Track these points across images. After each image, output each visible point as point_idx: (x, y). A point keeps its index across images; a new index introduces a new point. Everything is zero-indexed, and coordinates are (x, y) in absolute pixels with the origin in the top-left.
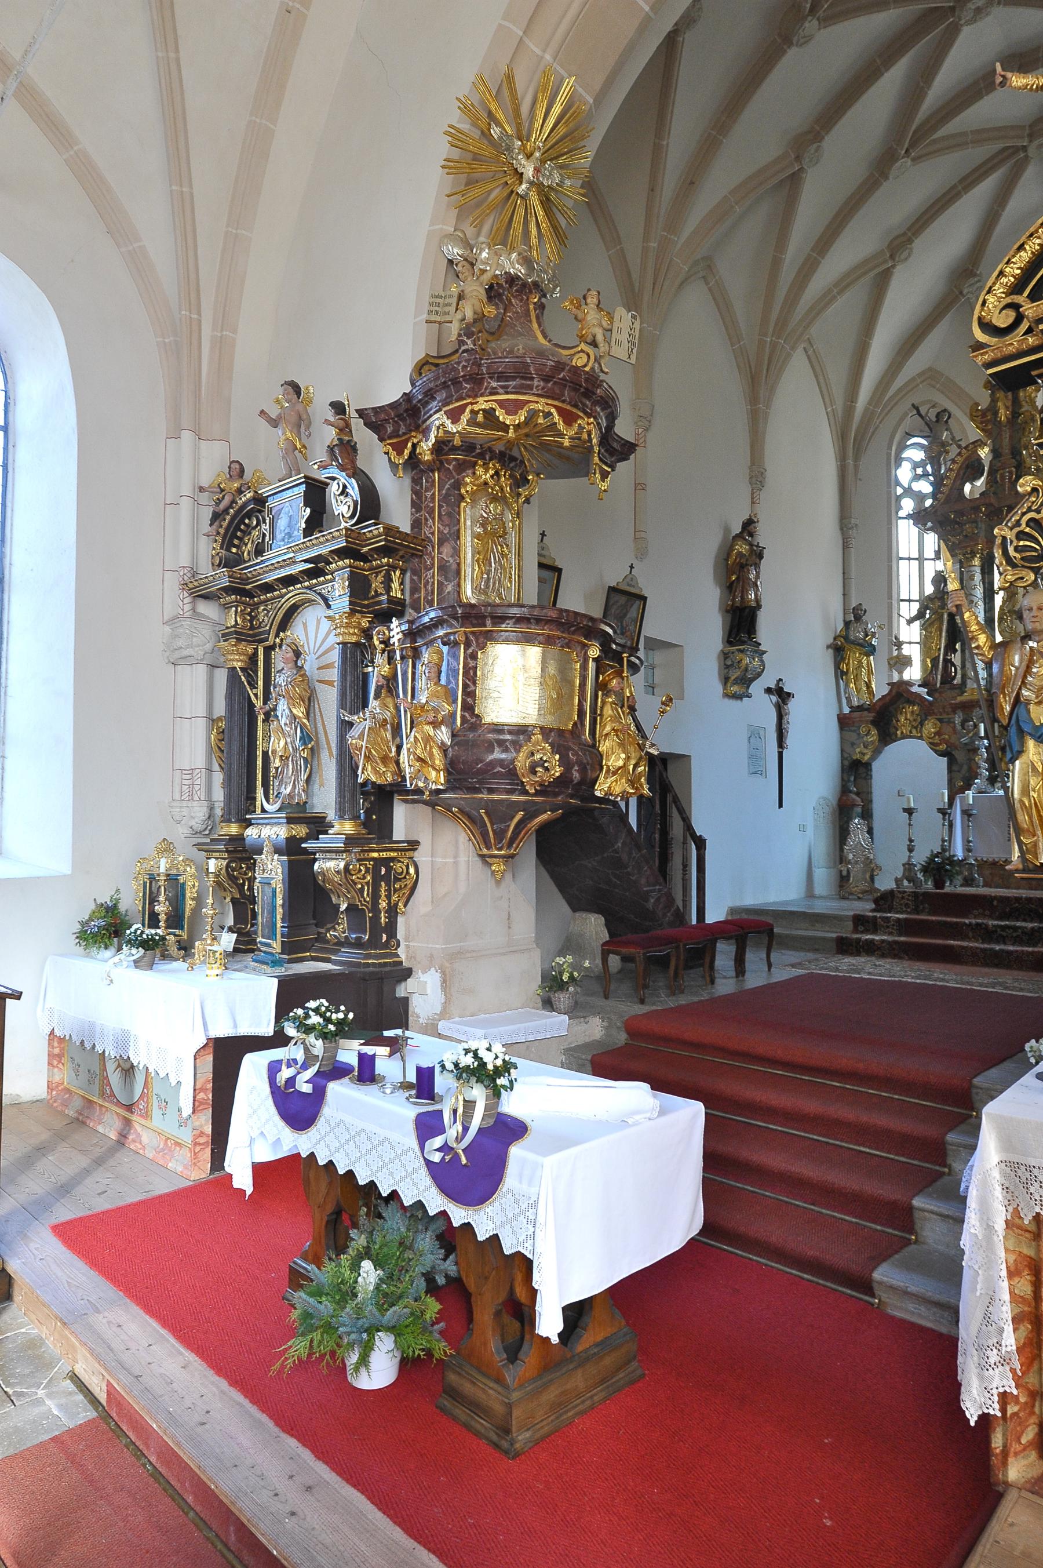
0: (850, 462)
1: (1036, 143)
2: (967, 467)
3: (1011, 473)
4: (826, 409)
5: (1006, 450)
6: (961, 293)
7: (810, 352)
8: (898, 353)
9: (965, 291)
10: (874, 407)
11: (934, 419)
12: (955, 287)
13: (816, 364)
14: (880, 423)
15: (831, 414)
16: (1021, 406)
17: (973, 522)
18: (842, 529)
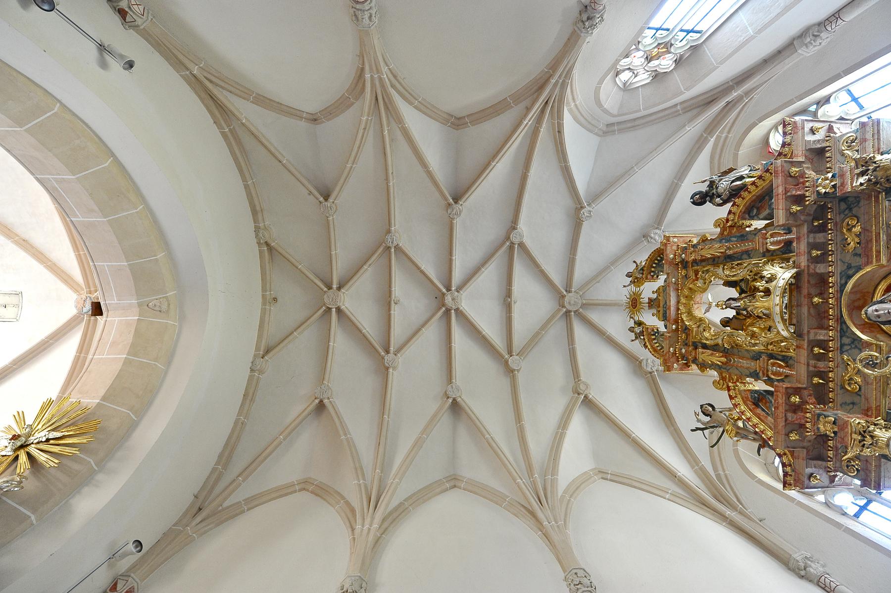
0: (728, 512)
1: (566, 304)
2: (756, 405)
3: (773, 365)
4: (665, 498)
5: (753, 365)
6: (651, 373)
7: (609, 477)
8: (668, 428)
9: (649, 370)
10: (698, 465)
11: (708, 419)
12: (646, 375)
13: (625, 481)
14: (724, 471)
15: (672, 498)
16: (717, 345)
17: (818, 419)
18: (802, 577)
